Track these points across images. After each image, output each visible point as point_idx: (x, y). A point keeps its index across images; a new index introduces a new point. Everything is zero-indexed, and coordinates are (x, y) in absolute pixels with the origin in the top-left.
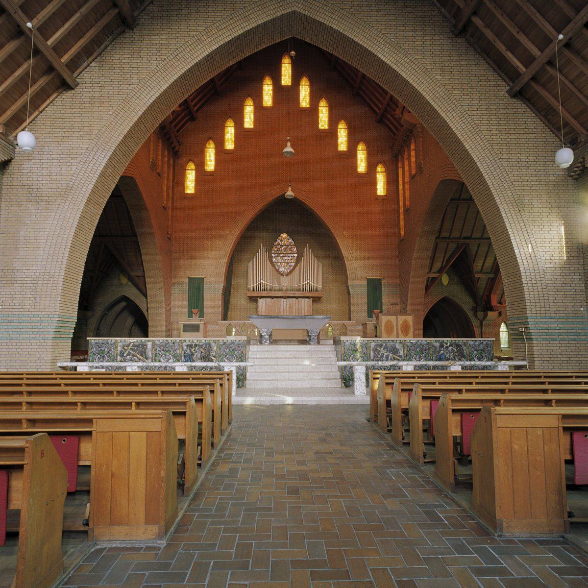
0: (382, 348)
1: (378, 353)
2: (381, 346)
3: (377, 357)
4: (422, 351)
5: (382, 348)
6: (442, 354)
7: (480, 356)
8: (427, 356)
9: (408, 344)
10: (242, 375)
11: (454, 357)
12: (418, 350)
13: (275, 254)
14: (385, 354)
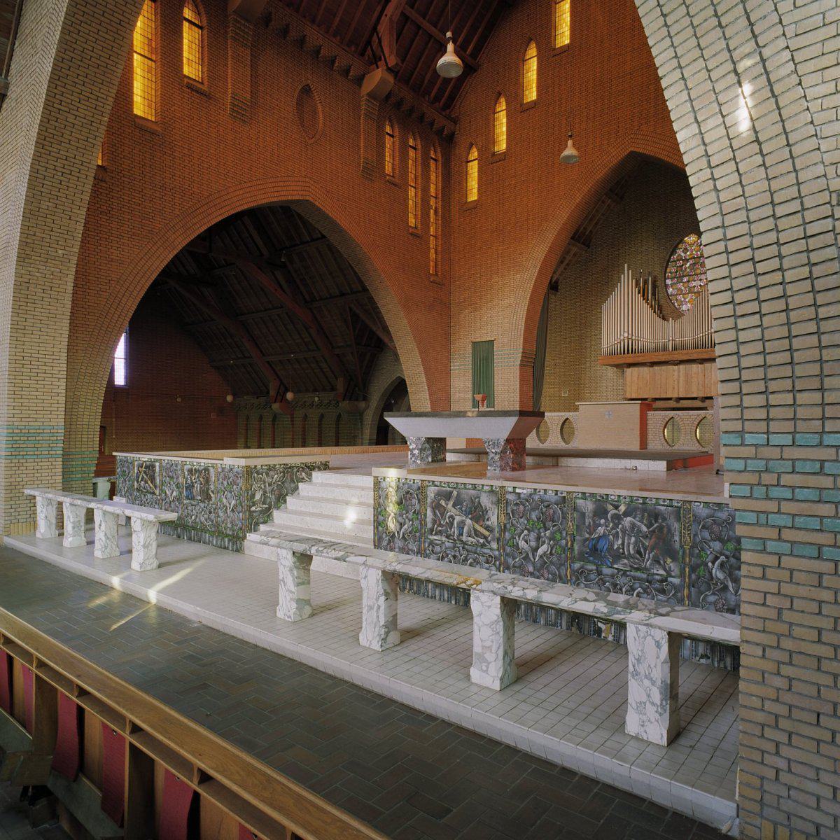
0: (451, 503)
1: (442, 515)
2: (448, 496)
3: (440, 525)
4: (544, 521)
5: (451, 503)
6: (600, 537)
7: (733, 560)
8: (558, 536)
9: (511, 497)
11: (639, 552)
12: (534, 516)
13: (672, 279)
14: (458, 519)
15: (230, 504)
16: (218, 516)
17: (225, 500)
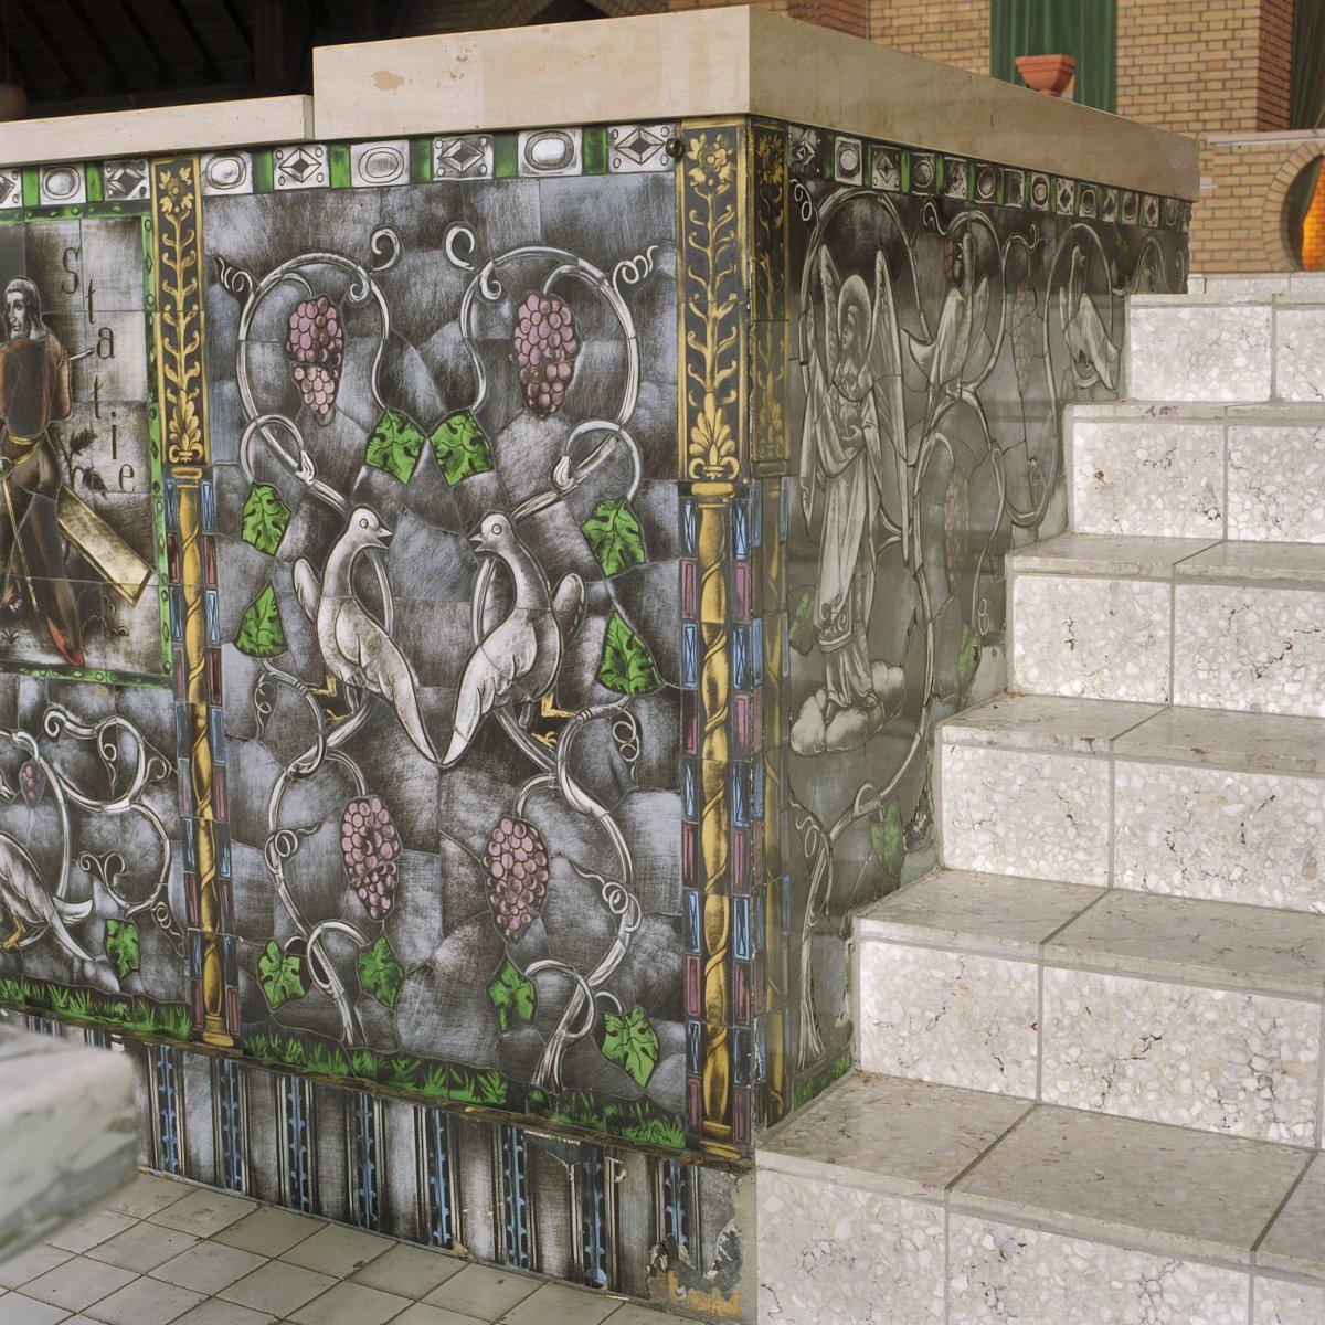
10: (666, 1001)
15: (441, 675)
16: (240, 826)
17: (340, 629)
